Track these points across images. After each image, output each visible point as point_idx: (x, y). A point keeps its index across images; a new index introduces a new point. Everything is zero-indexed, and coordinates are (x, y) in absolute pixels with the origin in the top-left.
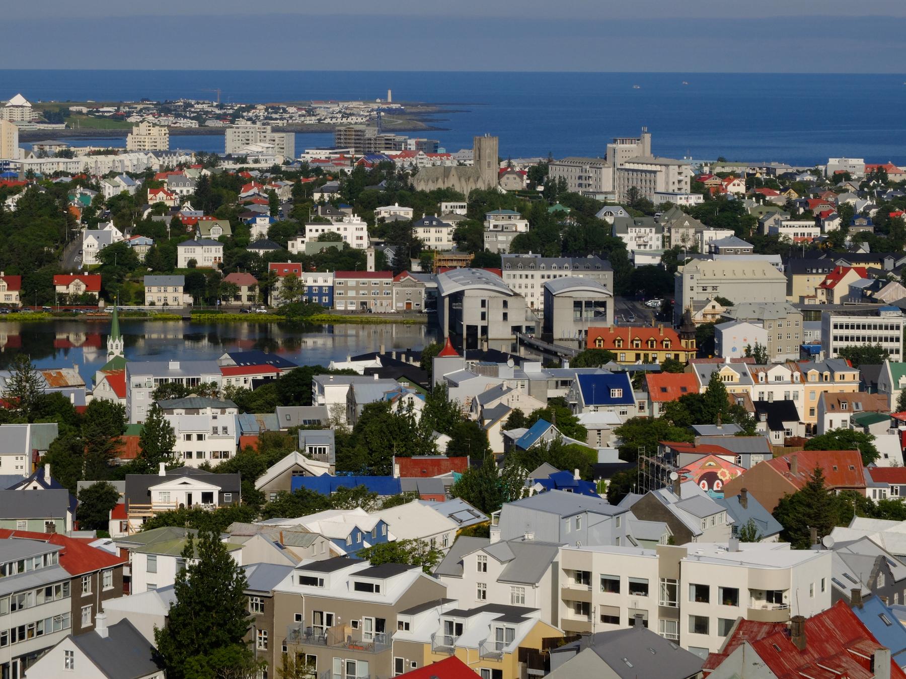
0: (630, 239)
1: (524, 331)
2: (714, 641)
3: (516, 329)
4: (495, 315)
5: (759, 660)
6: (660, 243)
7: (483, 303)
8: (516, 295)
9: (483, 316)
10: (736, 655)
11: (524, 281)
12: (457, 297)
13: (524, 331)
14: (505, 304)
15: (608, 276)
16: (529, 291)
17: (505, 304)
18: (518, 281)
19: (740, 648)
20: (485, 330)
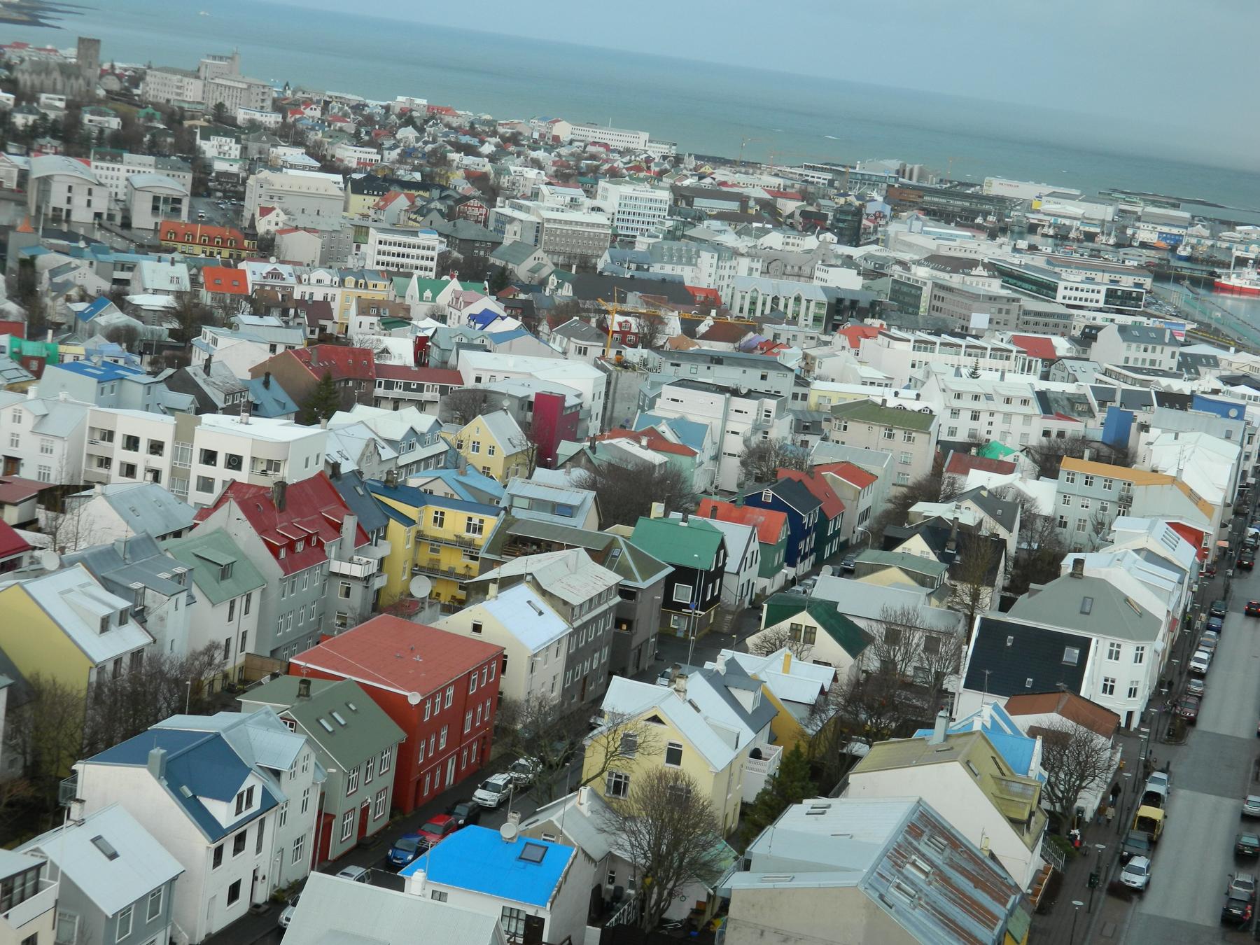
0: (209, 147)
1: (105, 217)
2: (209, 499)
3: (98, 215)
4: (80, 200)
5: (242, 516)
6: (238, 153)
7: (70, 189)
8: (100, 184)
9: (69, 200)
10: (224, 509)
11: (110, 173)
12: (45, 181)
13: (105, 217)
14: (90, 192)
15: (189, 177)
16: (114, 182)
17: (90, 192)
18: (105, 172)
19: (227, 504)
20: (69, 212)
